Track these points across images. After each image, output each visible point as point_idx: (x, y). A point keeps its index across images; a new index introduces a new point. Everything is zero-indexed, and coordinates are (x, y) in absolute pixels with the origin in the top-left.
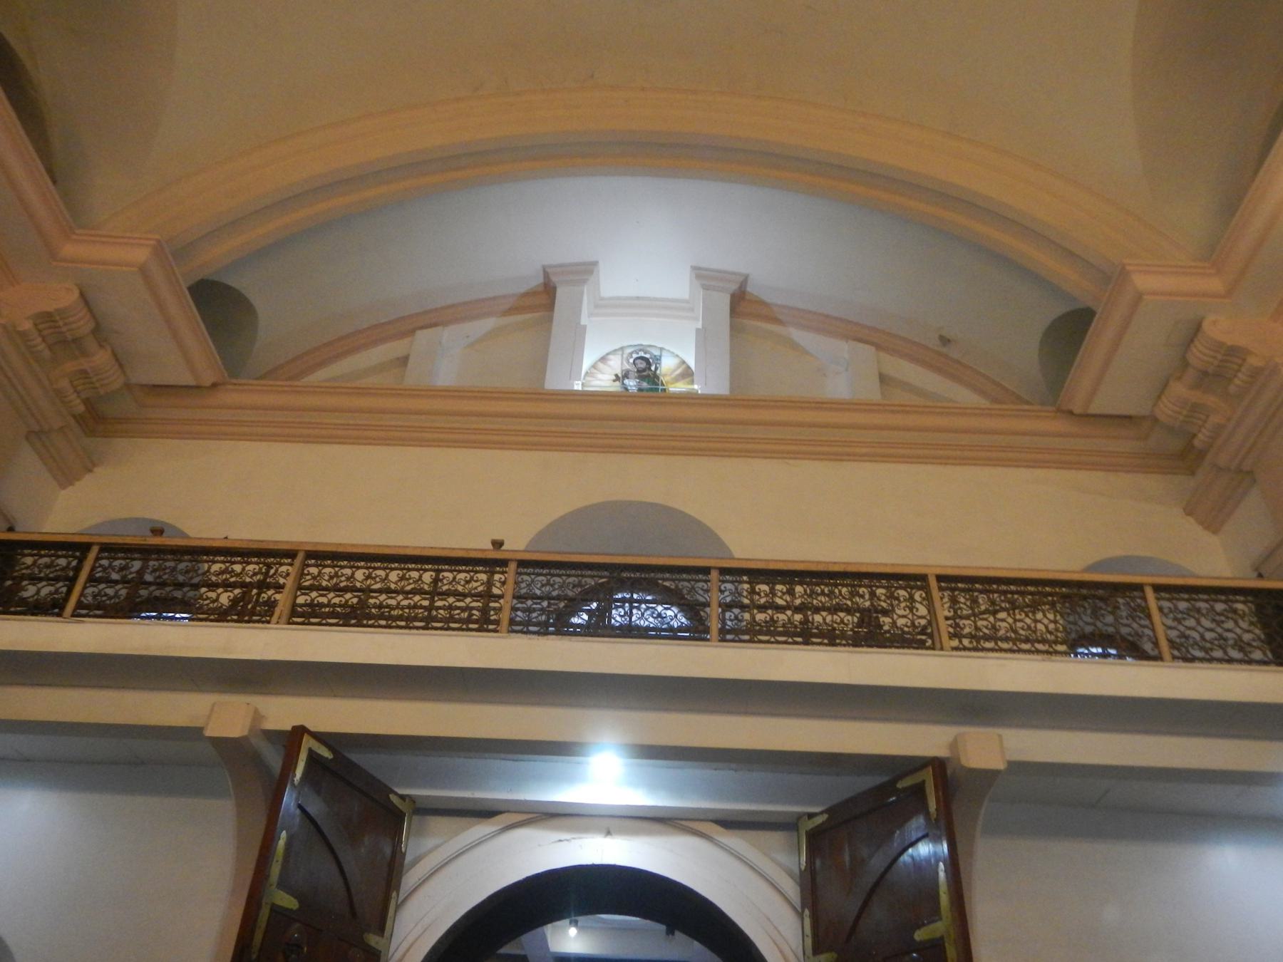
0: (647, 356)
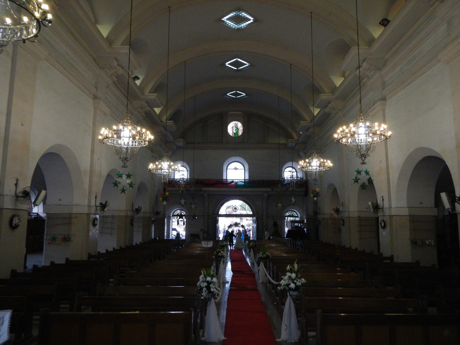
0: (236, 123)
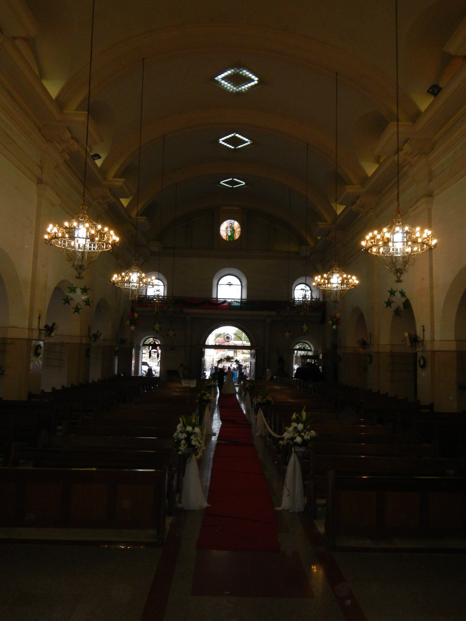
0: (232, 222)
